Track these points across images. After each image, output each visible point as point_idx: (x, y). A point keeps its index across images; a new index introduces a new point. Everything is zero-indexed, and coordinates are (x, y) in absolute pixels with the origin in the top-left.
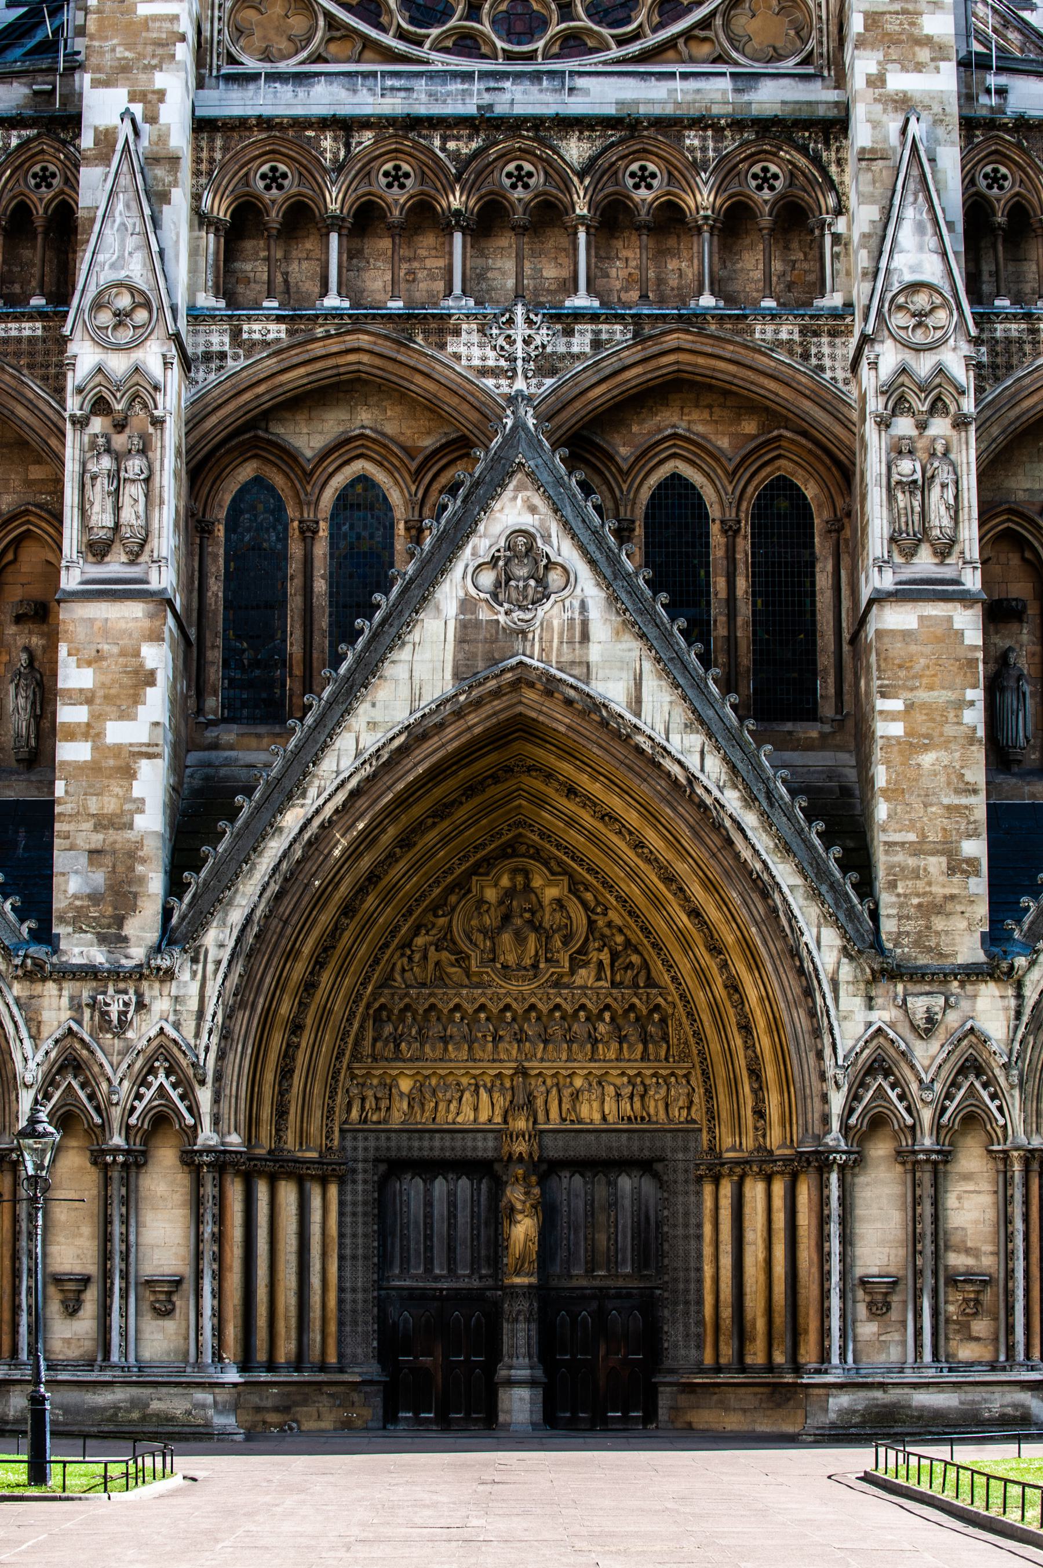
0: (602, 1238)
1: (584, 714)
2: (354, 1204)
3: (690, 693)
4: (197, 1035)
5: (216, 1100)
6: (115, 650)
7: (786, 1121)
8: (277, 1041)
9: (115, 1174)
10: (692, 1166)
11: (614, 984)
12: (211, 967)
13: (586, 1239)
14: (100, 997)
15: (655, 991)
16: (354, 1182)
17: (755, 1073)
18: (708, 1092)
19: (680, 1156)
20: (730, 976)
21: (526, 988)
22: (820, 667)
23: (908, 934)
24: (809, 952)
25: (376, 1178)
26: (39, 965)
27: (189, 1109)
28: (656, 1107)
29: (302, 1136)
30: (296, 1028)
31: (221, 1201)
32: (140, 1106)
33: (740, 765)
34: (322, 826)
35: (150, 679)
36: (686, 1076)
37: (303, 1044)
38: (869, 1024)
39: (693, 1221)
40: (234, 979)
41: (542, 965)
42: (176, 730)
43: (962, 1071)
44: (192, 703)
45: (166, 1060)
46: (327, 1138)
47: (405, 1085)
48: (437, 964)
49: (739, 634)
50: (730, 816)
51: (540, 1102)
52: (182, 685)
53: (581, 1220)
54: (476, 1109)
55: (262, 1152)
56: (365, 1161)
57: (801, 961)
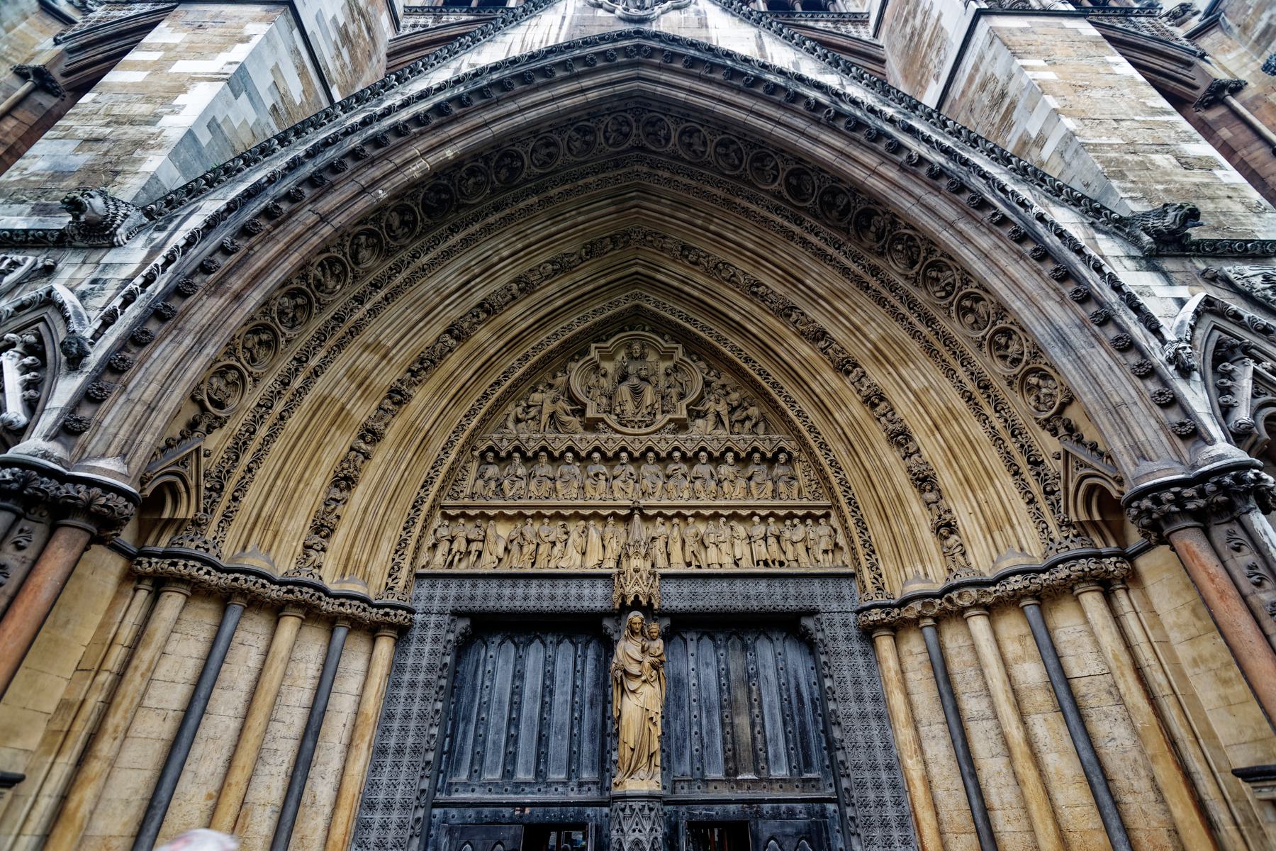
10: (852, 617)
13: (723, 724)
15: (776, 437)
16: (422, 640)
19: (834, 606)
25: (451, 637)
30: (371, 435)
36: (827, 516)
37: (377, 459)
41: (659, 417)
46: (390, 575)
47: (504, 530)
48: (552, 416)
53: (714, 697)
54: (584, 554)
56: (440, 613)
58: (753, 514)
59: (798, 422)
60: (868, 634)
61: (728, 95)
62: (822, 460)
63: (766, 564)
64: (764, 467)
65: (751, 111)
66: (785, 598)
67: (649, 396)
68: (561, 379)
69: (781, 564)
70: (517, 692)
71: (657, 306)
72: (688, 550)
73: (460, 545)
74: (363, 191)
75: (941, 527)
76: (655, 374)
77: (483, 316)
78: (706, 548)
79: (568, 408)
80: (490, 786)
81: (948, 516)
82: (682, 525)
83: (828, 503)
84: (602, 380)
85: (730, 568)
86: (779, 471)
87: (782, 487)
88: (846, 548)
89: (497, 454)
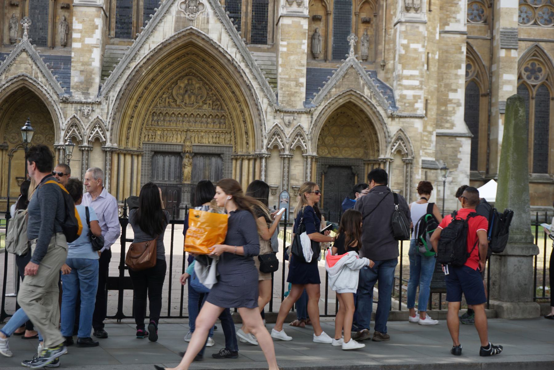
0: (207, 173)
1: (207, 42)
2: (145, 162)
3: (234, 38)
4: (107, 118)
5: (111, 135)
6: (88, 19)
7: (254, 145)
8: (127, 120)
9: (85, 153)
11: (213, 109)
12: (111, 102)
14: (82, 108)
15: (223, 111)
16: (145, 156)
17: (246, 133)
19: (228, 153)
20: (241, 109)
21: (191, 109)
22: (268, 30)
23: (285, 101)
26: (67, 99)
27: (104, 137)
29: (133, 145)
30: (132, 117)
31: (111, 160)
32: (92, 136)
33: (245, 57)
34: (140, 67)
35: (97, 28)
36: (230, 133)
38: (274, 123)
39: (230, 169)
40: (117, 104)
41: (195, 103)
42: (103, 40)
43: (297, 135)
44: (107, 32)
47: (159, 133)
48: (168, 102)
49: (248, 21)
50: (242, 69)
51: (193, 139)
52: (105, 28)
54: (177, 139)
55: (122, 148)
56: (149, 151)
65: (216, 54)
66: (218, 151)
67: (193, 98)
68: (170, 91)
70: (164, 165)
72: (199, 139)
73: (150, 136)
76: (195, 88)
79: (172, 101)
80: (160, 181)
85: (207, 144)
87: (221, 126)
89: (156, 114)
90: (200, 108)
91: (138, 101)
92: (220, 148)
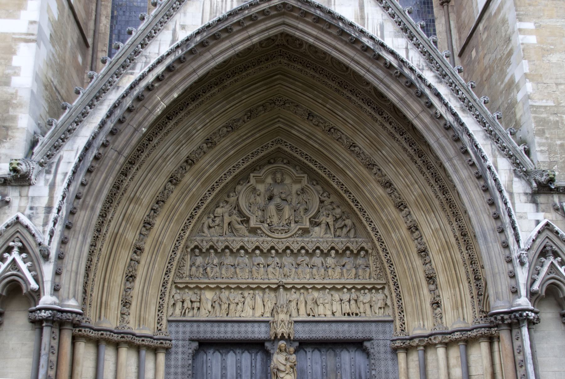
12: (59, 177)
15: (360, 240)
18: (398, 295)
24: (492, 173)
28: (364, 307)
36: (383, 288)
38: (538, 222)
41: (293, 225)
45: (21, 242)
48: (229, 224)
51: (293, 304)
57: (486, 181)
58: (344, 287)
59: (372, 234)
60: (395, 351)
61: (339, 46)
62: (383, 258)
63: (349, 314)
64: (352, 259)
67: (287, 212)
68: (232, 199)
69: (357, 314)
71: (292, 150)
72: (309, 307)
74: (136, 130)
75: (434, 303)
76: (290, 194)
77: (188, 167)
78: (318, 305)
79: (239, 219)
81: (437, 299)
82: (305, 293)
83: (384, 281)
84: (258, 198)
86: (360, 261)
87: (360, 272)
88: (391, 307)
89: (201, 250)
90: (306, 231)
91: (155, 210)
92: (360, 325)
